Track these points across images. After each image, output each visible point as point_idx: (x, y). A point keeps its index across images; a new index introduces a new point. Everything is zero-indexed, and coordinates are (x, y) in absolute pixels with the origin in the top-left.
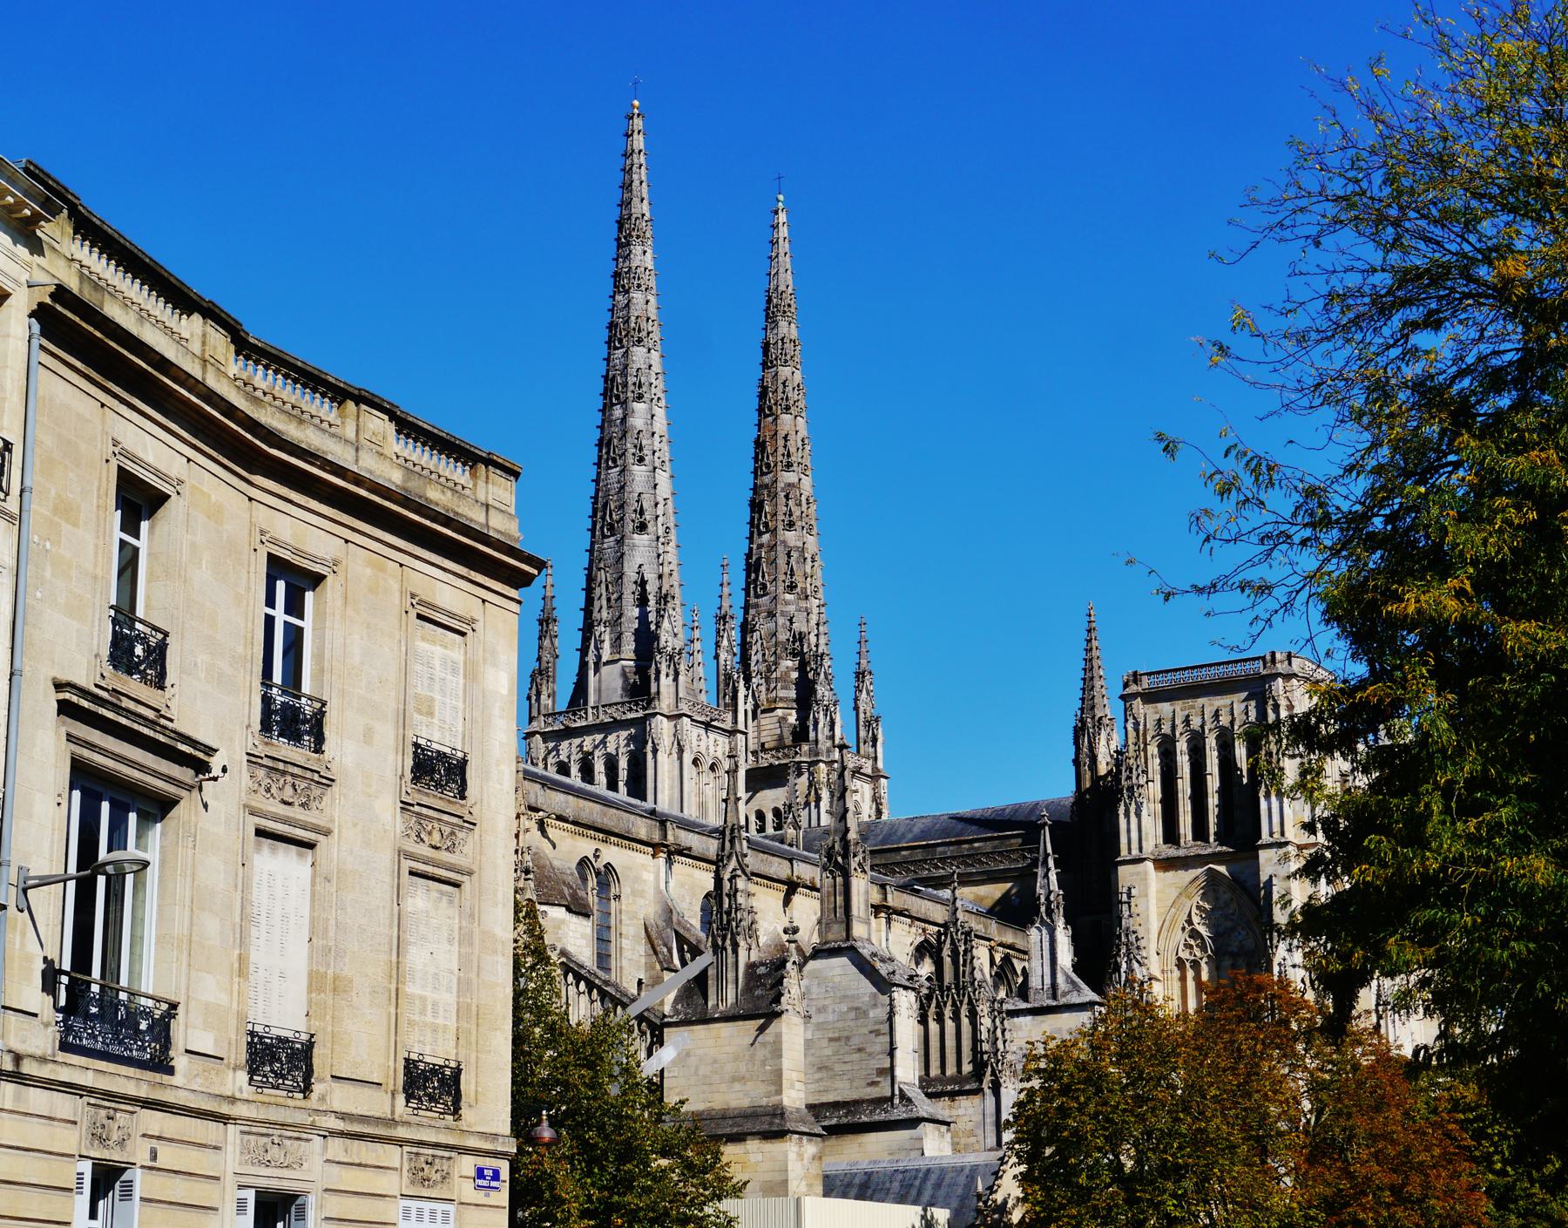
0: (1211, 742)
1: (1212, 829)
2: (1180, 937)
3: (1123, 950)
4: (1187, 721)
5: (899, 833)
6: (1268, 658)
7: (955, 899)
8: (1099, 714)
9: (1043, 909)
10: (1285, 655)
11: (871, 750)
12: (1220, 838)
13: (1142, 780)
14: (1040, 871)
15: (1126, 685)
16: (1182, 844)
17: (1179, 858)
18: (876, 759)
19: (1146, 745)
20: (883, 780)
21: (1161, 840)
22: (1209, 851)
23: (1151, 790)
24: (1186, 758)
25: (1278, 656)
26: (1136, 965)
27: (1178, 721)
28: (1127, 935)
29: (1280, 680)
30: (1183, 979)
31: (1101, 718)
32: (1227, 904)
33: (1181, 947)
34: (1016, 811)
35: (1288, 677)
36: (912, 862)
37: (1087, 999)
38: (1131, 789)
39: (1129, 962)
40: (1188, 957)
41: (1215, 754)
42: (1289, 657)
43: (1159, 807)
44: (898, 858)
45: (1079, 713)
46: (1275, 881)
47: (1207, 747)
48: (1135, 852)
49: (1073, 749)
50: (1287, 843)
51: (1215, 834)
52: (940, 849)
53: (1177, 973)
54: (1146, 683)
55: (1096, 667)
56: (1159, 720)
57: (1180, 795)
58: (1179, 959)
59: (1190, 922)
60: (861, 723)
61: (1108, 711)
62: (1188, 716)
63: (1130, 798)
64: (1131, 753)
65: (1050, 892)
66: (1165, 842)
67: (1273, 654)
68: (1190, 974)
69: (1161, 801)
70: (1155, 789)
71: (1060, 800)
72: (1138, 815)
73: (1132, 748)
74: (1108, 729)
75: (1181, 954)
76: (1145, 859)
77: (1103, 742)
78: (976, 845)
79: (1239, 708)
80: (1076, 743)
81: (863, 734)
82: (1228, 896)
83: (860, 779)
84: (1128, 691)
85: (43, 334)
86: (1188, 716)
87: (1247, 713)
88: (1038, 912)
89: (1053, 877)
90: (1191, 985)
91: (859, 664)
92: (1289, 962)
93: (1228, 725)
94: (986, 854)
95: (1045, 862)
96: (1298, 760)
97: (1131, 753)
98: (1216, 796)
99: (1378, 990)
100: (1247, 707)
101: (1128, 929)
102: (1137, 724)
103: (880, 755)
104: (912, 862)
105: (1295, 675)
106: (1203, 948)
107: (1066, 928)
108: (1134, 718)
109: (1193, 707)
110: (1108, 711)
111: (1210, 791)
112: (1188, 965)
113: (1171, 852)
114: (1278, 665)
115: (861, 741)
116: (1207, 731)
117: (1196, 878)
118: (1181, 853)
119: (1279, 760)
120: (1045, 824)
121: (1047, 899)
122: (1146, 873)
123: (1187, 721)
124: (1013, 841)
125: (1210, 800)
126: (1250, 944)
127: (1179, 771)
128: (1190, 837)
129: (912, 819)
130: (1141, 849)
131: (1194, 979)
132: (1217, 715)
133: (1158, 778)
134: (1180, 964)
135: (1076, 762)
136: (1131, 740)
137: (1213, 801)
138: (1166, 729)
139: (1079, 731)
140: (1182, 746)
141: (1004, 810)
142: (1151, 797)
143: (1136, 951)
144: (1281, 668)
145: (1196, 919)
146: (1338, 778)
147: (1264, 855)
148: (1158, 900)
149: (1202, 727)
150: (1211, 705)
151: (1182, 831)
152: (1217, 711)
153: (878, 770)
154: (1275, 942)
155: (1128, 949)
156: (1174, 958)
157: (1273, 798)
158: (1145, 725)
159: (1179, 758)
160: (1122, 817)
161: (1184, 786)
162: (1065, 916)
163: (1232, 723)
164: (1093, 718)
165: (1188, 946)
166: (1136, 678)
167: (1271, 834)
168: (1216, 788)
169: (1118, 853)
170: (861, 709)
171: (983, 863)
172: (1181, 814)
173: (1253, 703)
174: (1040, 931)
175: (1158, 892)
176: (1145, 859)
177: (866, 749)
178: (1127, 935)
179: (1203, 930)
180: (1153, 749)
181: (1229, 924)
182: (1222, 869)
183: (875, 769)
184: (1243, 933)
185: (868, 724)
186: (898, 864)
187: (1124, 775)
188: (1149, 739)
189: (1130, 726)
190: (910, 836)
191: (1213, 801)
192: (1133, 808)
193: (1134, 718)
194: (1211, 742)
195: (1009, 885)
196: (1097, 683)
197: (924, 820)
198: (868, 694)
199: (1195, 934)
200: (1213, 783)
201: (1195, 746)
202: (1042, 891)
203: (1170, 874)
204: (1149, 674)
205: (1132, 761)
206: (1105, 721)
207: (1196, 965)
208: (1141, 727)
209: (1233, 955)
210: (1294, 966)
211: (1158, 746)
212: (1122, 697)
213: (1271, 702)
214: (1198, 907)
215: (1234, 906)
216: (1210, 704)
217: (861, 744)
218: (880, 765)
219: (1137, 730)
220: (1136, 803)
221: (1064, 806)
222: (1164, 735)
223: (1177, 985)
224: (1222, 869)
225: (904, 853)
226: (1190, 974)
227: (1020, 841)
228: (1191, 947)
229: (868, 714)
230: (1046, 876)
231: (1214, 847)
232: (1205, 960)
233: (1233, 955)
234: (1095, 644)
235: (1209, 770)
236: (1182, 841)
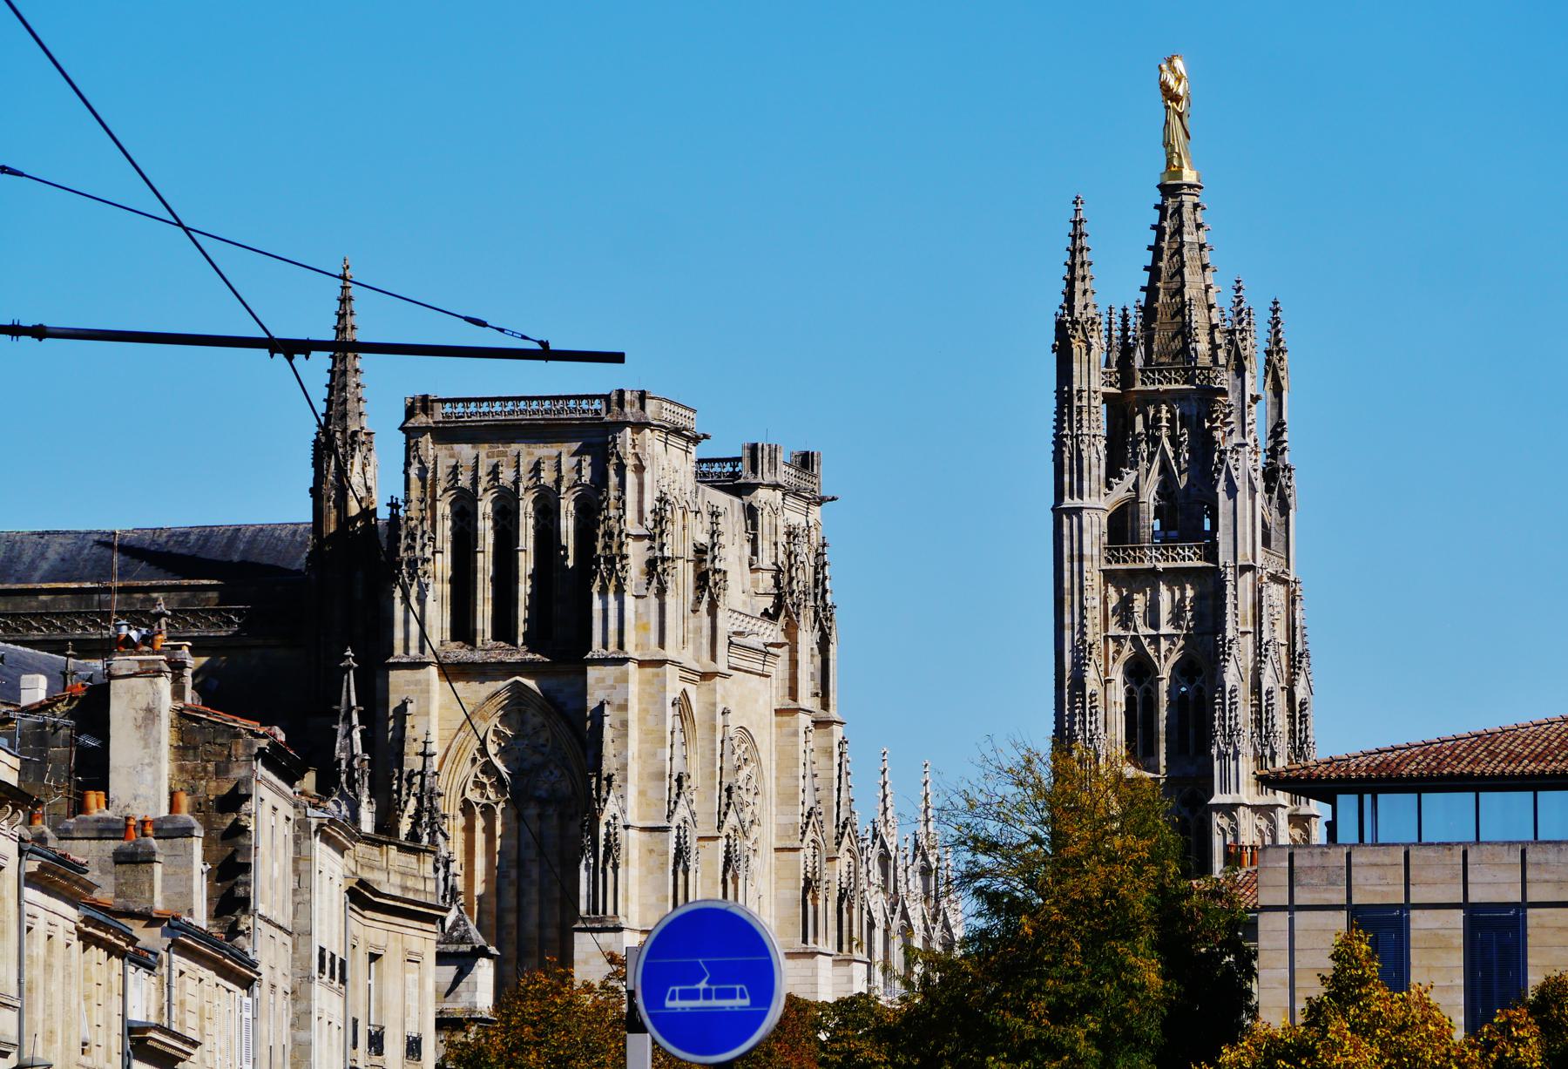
0: (527, 505)
1: (522, 628)
2: (467, 771)
3: (425, 819)
4: (494, 473)
5: (26, 558)
6: (614, 398)
8: (353, 427)
9: (343, 778)
12: (532, 643)
13: (428, 552)
14: (341, 728)
15: (410, 412)
16: (479, 643)
17: (473, 663)
19: (434, 500)
21: (447, 635)
22: (517, 657)
23: (439, 565)
24: (490, 524)
25: (628, 396)
26: (440, 838)
27: (482, 472)
28: (431, 799)
29: (628, 430)
30: (469, 829)
31: (355, 433)
32: (536, 732)
33: (470, 785)
35: (639, 426)
36: (58, 615)
38: (412, 564)
39: (432, 836)
40: (479, 800)
41: (531, 522)
42: (643, 396)
43: (447, 588)
44: (33, 604)
46: (607, 710)
48: (414, 651)
49: (311, 472)
50: (626, 660)
51: (524, 634)
53: (461, 821)
54: (440, 412)
56: (455, 468)
57: (480, 576)
58: (466, 802)
59: (483, 751)
61: (365, 422)
62: (496, 466)
63: (412, 576)
64: (414, 513)
66: (454, 639)
67: (621, 393)
68: (480, 823)
69: (452, 581)
70: (443, 564)
71: (274, 527)
72: (422, 601)
73: (415, 505)
74: (364, 448)
75: (468, 795)
76: (429, 664)
77: (357, 468)
79: (568, 463)
80: (318, 463)
82: (538, 720)
84: (413, 423)
85: (351, 901)
86: (496, 466)
87: (579, 471)
88: (337, 782)
89: (357, 735)
90: (480, 838)
92: (620, 822)
95: (348, 718)
96: (647, 543)
97: (414, 513)
98: (529, 582)
99: (727, 852)
100: (579, 463)
101: (432, 790)
104: (58, 615)
105: (648, 425)
106: (500, 785)
107: (370, 802)
108: (421, 462)
109: (504, 454)
110: (365, 422)
111: (522, 574)
112: (477, 810)
113: (460, 653)
114: (627, 409)
116: (522, 490)
117: (497, 694)
118: (478, 656)
119: (621, 544)
120: (350, 667)
121: (350, 764)
123: (494, 473)
125: (521, 587)
126: (565, 787)
127: (480, 543)
128: (488, 635)
129: (42, 534)
130: (422, 649)
131: (484, 830)
132: (536, 469)
133: (448, 547)
134: (467, 808)
135: (316, 492)
136: (415, 493)
137: (524, 588)
138: (464, 480)
140: (485, 506)
141: (186, 534)
142: (439, 575)
143: (440, 820)
144: (631, 412)
145: (492, 749)
146: (691, 554)
147: (593, 673)
148: (441, 718)
149: (516, 482)
151: (479, 626)
152: (538, 463)
154: (604, 794)
155: (431, 817)
156: (459, 800)
157: (611, 597)
158: (435, 472)
159: (480, 524)
161: (485, 563)
162: (370, 789)
163: (558, 481)
164: (344, 431)
165: (479, 785)
166: (425, 404)
167: (605, 645)
168: (529, 571)
169: (391, 654)
173: (588, 459)
175: (441, 707)
176: (429, 664)
179: (498, 763)
180: (444, 508)
181: (537, 758)
182: (531, 683)
184: (557, 772)
186: (34, 616)
187: (403, 544)
188: (439, 492)
189: (413, 472)
190: (45, 566)
191: (524, 588)
192: (414, 591)
193: (421, 462)
194: (527, 505)
196: (352, 381)
197: (60, 539)
199: (489, 768)
200: (526, 563)
202: (343, 755)
204: (444, 401)
205: (412, 524)
206: (362, 437)
207: (488, 811)
209: (541, 802)
210: (626, 827)
211: (452, 504)
212: (402, 428)
213: (614, 460)
214: (496, 733)
215: (545, 735)
216: (530, 453)
219: (422, 478)
220: (420, 585)
221: (279, 538)
222: (462, 489)
224: (531, 683)
226: (480, 823)
227: (214, 595)
230: (349, 735)
231: (520, 654)
232: (502, 805)
233: (541, 802)
234: (350, 320)
235: (521, 545)
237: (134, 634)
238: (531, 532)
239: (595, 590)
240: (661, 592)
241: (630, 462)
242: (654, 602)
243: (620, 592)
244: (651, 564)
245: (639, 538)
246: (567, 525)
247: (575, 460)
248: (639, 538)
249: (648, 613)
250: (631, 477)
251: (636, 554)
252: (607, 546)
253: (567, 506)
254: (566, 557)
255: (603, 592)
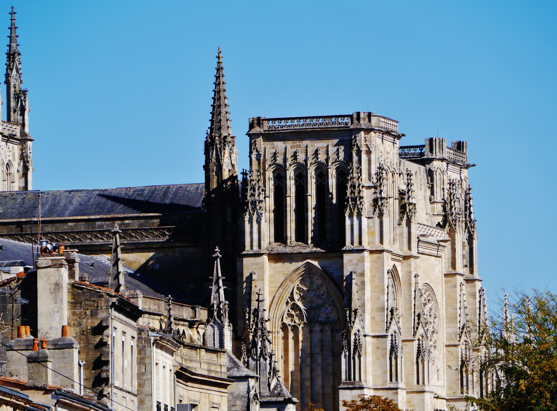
0: (311, 172)
2: (284, 308)
4: (295, 156)
5: (62, 204)
6: (355, 116)
7: (170, 316)
8: (224, 134)
9: (215, 313)
10: (366, 114)
11: (20, 118)
14: (214, 288)
15: (251, 126)
16: (289, 243)
17: (286, 254)
18: (23, 125)
19: (265, 170)
20: (29, 143)
21: (273, 239)
22: (308, 250)
23: (267, 203)
24: (293, 182)
25: (362, 115)
26: (267, 343)
27: (289, 156)
28: (262, 323)
29: (362, 133)
30: (286, 338)
32: (318, 288)
33: (285, 315)
34: (153, 192)
35: (368, 131)
36: (77, 233)
37: (243, 374)
38: (254, 203)
39: (263, 341)
41: (314, 181)
42: (369, 115)
43: (272, 215)
44: (65, 228)
45: (209, 130)
46: (354, 276)
47: (309, 176)
48: (255, 248)
50: (363, 250)
52: (98, 223)
53: (281, 334)
54: (266, 126)
55: (222, 97)
57: (288, 209)
58: (284, 324)
59: (292, 298)
60: (12, 96)
61: (231, 131)
62: (295, 153)
65: (220, 302)
66: (276, 240)
67: (358, 114)
68: (291, 335)
70: (270, 203)
72: (259, 222)
73: (255, 173)
74: (230, 145)
75: (285, 321)
76: (263, 254)
77: (227, 155)
78: (127, 222)
79: (332, 149)
80: (207, 153)
81: (13, 104)
82: (319, 282)
83: (12, 142)
84: (253, 131)
86: (295, 153)
87: (338, 154)
89: (222, 292)
91: (10, 46)
93: (324, 161)
94: (134, 230)
95: (217, 282)
98: (313, 211)
99: (419, 348)
100: (338, 150)
101: (262, 319)
102: (259, 155)
103: (27, 122)
104: (77, 233)
106: (301, 317)
107: (229, 326)
108: (257, 151)
110: (231, 131)
111: (309, 207)
112: (290, 328)
113: (280, 248)
114: (362, 122)
115: (12, 110)
116: (309, 164)
117: (298, 269)
118: (288, 250)
119: (360, 191)
120: (218, 257)
121: (218, 306)
122: (263, 264)
123: (295, 156)
124: (154, 221)
128: (293, 238)
129: (70, 192)
132: (316, 153)
133: (272, 194)
134: (284, 327)
137: (311, 214)
138: (280, 160)
139: (209, 145)
140: (290, 173)
141: (143, 190)
144: (363, 123)
145: (296, 297)
146: (397, 195)
147: (346, 257)
148: (270, 282)
149: (306, 161)
150: (312, 146)
151: (289, 235)
153: (26, 135)
155: (262, 333)
156: (280, 323)
157: (355, 218)
159: (288, 182)
160: (247, 223)
161: (291, 202)
162: (229, 318)
163: (327, 160)
164: (220, 136)
167: (352, 243)
168: (313, 206)
170: (12, 84)
171: (132, 236)
172: (288, 222)
173: (342, 148)
174: (214, 328)
176: (263, 254)
177: (14, 116)
178: (262, 323)
179: (300, 304)
180: (270, 174)
181: (320, 301)
182: (316, 263)
183: (23, 133)
185: (18, 97)
186: (66, 233)
188: (267, 166)
189: (254, 156)
190: (71, 208)
191: (311, 214)
192: (255, 217)
193: (257, 151)
194: (311, 172)
195: (152, 254)
197: (79, 194)
198: (17, 71)
199: (295, 307)
200: (312, 202)
201: (300, 173)
202: (215, 302)
203: (279, 265)
207: (295, 329)
208: (262, 158)
209: (322, 323)
213: (355, 148)
214: (298, 289)
216: (313, 145)
217: (12, 113)
218: (27, 130)
219: (258, 160)
223: (281, 342)
224: (316, 263)
225: (70, 224)
226: (291, 335)
228: (292, 316)
229: (17, 89)
230: (218, 291)
231: (310, 248)
232: (302, 326)
233: (322, 323)
236: (289, 241)
237: (49, 246)
238: (314, 186)
239: (347, 215)
240: (381, 215)
241: (364, 149)
242: (377, 220)
243: (359, 215)
244: (375, 201)
245: (369, 188)
246: (332, 182)
247: (336, 148)
248: (369, 188)
250: (364, 157)
251: (367, 196)
252: (352, 192)
253: (332, 172)
254: (332, 198)
255: (351, 216)
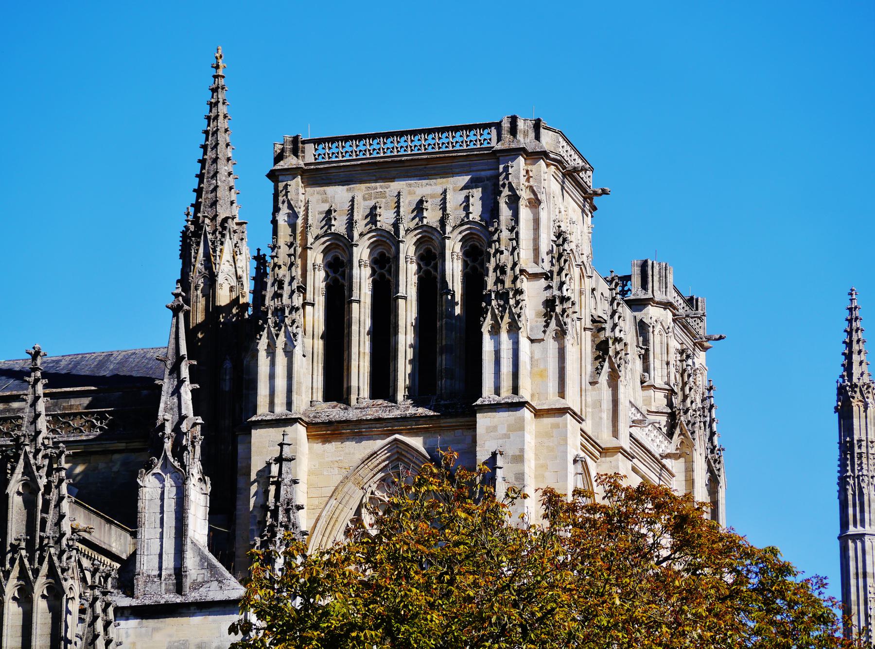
0: (408, 248)
4: (372, 216)
27: (358, 216)
87: (466, 208)
123: (372, 216)
132: (419, 207)
138: (339, 226)
157: (504, 336)
194: (408, 248)
213: (506, 192)
222: (336, 236)
238: (413, 279)
239: (486, 328)
240: (561, 333)
241: (525, 195)
242: (552, 346)
243: (514, 329)
244: (550, 304)
245: (535, 276)
248: (535, 276)
249: (545, 359)
250: (525, 213)
252: (499, 281)
253: (454, 246)
254: (453, 303)
255: (495, 331)
